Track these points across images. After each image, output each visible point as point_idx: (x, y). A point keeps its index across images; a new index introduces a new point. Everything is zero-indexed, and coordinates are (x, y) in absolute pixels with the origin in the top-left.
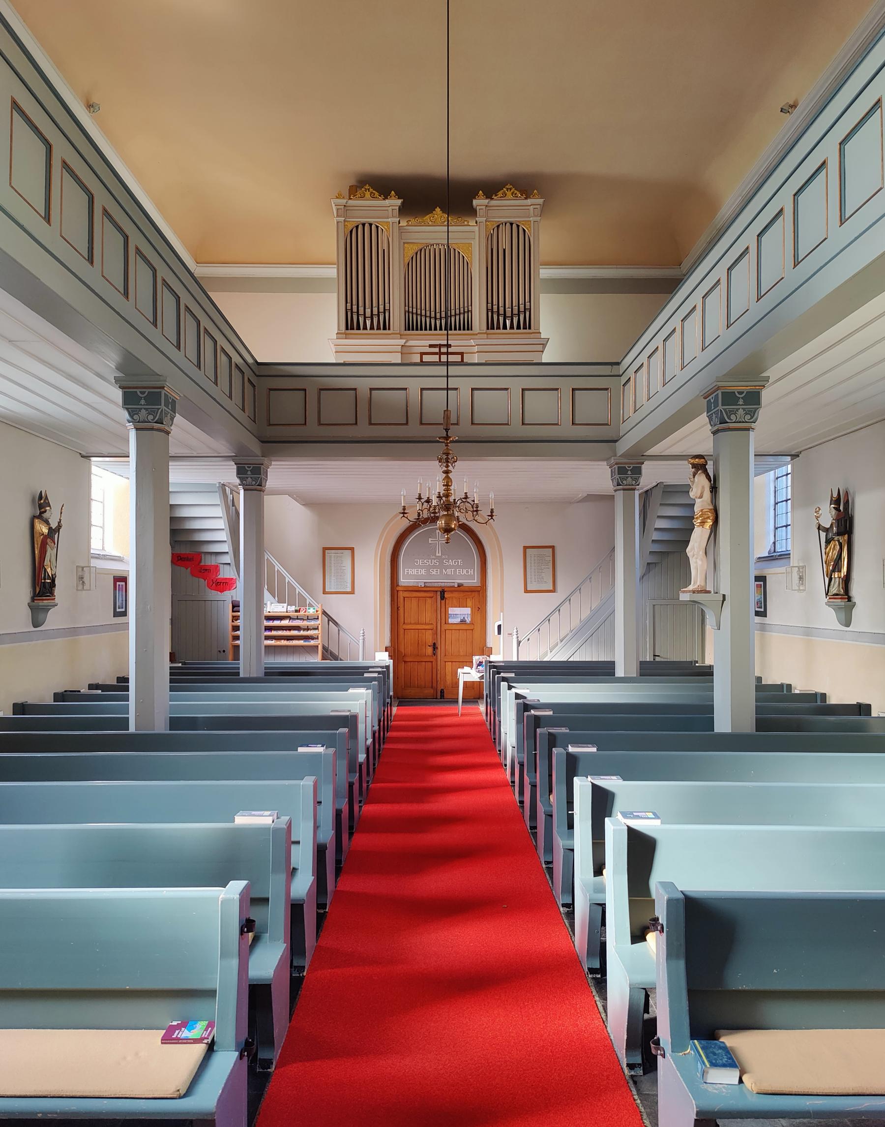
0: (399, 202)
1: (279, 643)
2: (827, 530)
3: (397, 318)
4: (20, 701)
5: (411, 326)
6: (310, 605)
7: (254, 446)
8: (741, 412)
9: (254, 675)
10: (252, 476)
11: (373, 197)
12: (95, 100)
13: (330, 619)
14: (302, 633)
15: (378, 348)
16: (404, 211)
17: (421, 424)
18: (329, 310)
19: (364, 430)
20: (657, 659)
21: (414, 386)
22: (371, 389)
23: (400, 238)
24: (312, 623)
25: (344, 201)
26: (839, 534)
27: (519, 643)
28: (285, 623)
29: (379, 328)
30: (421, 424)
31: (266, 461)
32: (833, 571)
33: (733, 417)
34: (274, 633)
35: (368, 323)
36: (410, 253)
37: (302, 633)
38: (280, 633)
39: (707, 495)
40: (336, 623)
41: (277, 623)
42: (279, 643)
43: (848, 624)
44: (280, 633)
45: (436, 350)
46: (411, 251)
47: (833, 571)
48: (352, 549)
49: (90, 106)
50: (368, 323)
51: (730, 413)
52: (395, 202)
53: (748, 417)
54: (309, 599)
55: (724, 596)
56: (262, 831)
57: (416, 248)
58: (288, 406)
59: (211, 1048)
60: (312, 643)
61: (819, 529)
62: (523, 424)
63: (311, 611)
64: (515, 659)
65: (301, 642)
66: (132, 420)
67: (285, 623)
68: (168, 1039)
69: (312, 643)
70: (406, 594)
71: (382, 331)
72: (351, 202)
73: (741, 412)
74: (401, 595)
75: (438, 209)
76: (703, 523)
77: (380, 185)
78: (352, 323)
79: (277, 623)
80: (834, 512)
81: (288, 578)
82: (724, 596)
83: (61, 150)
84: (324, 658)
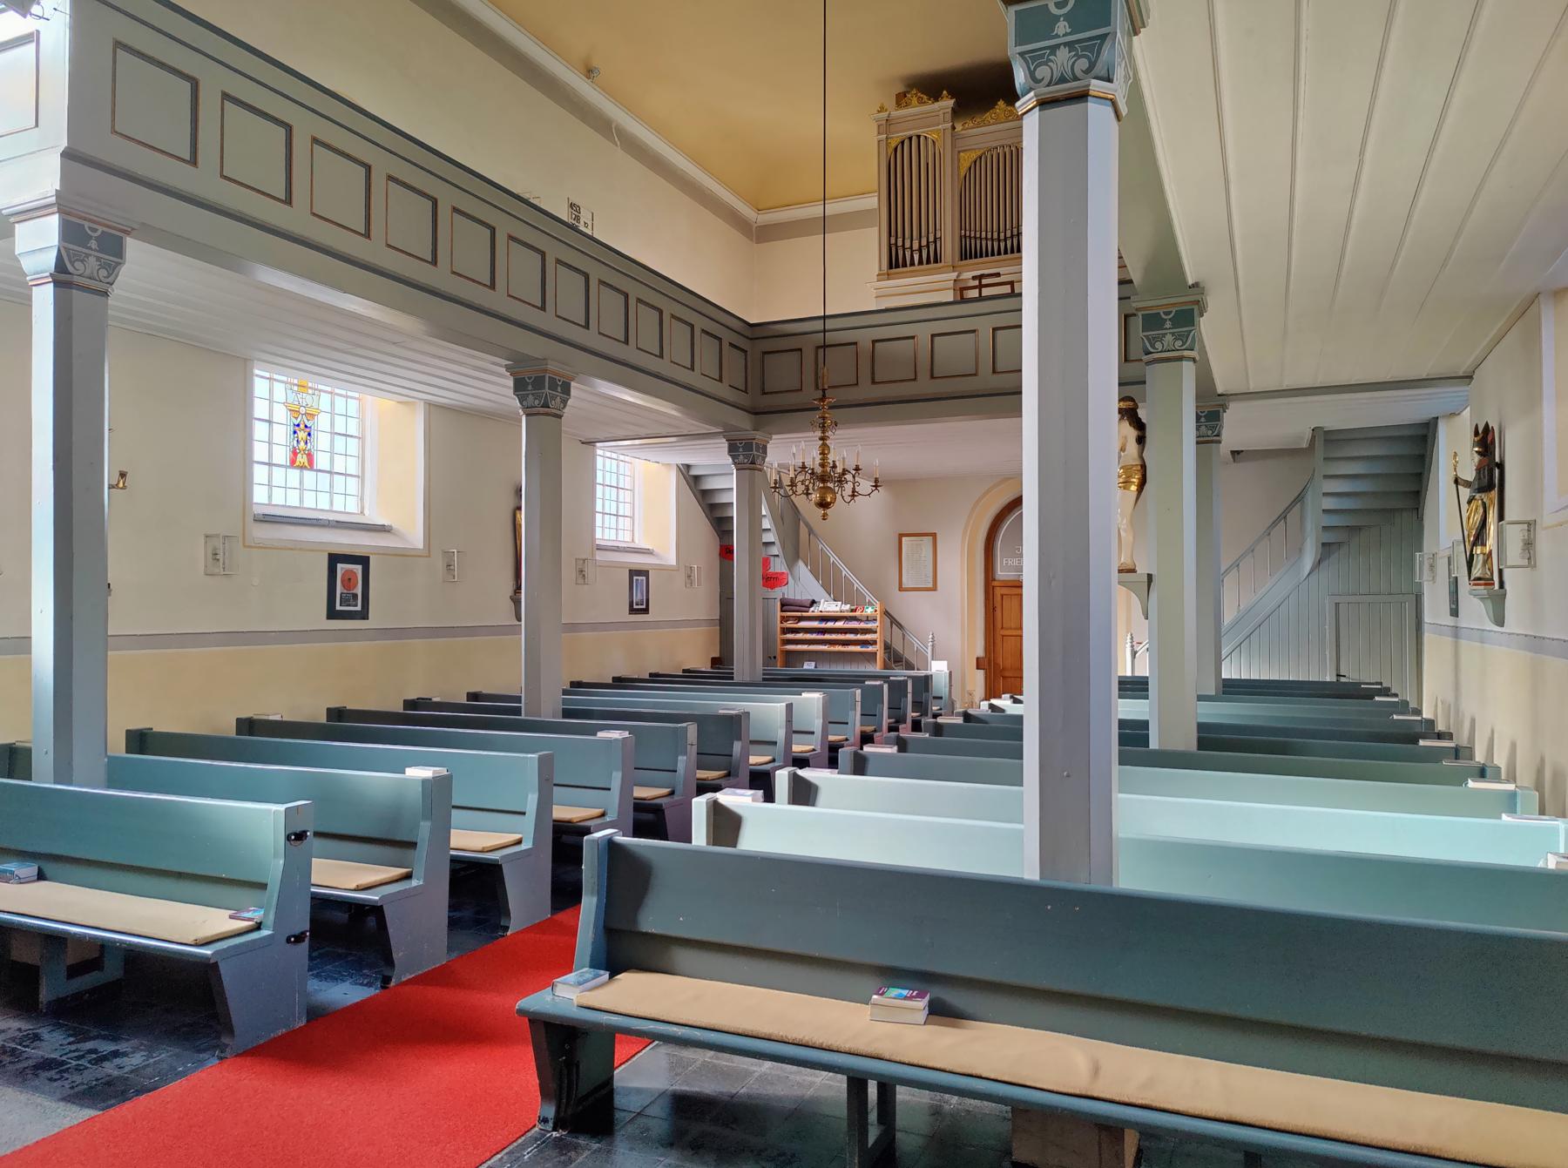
0: (951, 102)
1: (832, 648)
2: (1467, 484)
3: (949, 248)
4: (472, 690)
5: (966, 254)
6: (870, 604)
7: (743, 421)
8: (1169, 338)
9: (747, 679)
10: (747, 454)
11: (921, 102)
12: (595, 63)
13: (894, 621)
14: (859, 637)
15: (929, 286)
16: (957, 113)
17: (932, 377)
18: (868, 245)
19: (866, 391)
20: (1343, 680)
21: (923, 332)
22: (874, 342)
23: (953, 146)
24: (869, 625)
25: (884, 115)
26: (1480, 490)
27: (1134, 654)
28: (839, 624)
29: (928, 262)
30: (932, 377)
31: (759, 435)
32: (1474, 544)
33: (1158, 345)
34: (827, 637)
35: (916, 257)
36: (965, 165)
37: (859, 637)
38: (834, 637)
39: (1133, 447)
40: (900, 626)
41: (830, 625)
42: (832, 648)
43: (1500, 622)
44: (834, 637)
45: (976, 283)
46: (967, 159)
47: (1474, 544)
48: (934, 535)
49: (589, 72)
50: (916, 257)
51: (1152, 341)
52: (948, 103)
53: (1179, 343)
54: (869, 597)
55: (1150, 576)
56: (413, 780)
57: (974, 156)
58: (782, 372)
59: (258, 927)
60: (871, 649)
61: (1456, 481)
62: (994, 372)
63: (869, 611)
64: (1129, 674)
65: (858, 648)
66: (525, 408)
67: (839, 624)
68: (231, 917)
69: (871, 649)
70: (1005, 591)
71: (932, 265)
72: (895, 114)
73: (1169, 338)
74: (998, 592)
75: (1001, 103)
76: (1127, 483)
77: (930, 86)
78: (896, 262)
79: (830, 625)
80: (1477, 458)
81: (845, 572)
82: (1150, 576)
83: (383, 165)
84: (886, 667)
